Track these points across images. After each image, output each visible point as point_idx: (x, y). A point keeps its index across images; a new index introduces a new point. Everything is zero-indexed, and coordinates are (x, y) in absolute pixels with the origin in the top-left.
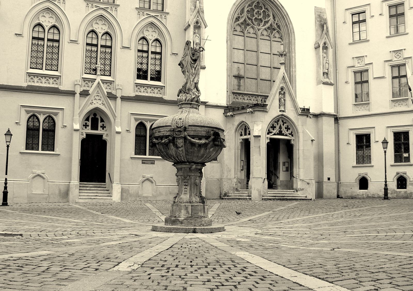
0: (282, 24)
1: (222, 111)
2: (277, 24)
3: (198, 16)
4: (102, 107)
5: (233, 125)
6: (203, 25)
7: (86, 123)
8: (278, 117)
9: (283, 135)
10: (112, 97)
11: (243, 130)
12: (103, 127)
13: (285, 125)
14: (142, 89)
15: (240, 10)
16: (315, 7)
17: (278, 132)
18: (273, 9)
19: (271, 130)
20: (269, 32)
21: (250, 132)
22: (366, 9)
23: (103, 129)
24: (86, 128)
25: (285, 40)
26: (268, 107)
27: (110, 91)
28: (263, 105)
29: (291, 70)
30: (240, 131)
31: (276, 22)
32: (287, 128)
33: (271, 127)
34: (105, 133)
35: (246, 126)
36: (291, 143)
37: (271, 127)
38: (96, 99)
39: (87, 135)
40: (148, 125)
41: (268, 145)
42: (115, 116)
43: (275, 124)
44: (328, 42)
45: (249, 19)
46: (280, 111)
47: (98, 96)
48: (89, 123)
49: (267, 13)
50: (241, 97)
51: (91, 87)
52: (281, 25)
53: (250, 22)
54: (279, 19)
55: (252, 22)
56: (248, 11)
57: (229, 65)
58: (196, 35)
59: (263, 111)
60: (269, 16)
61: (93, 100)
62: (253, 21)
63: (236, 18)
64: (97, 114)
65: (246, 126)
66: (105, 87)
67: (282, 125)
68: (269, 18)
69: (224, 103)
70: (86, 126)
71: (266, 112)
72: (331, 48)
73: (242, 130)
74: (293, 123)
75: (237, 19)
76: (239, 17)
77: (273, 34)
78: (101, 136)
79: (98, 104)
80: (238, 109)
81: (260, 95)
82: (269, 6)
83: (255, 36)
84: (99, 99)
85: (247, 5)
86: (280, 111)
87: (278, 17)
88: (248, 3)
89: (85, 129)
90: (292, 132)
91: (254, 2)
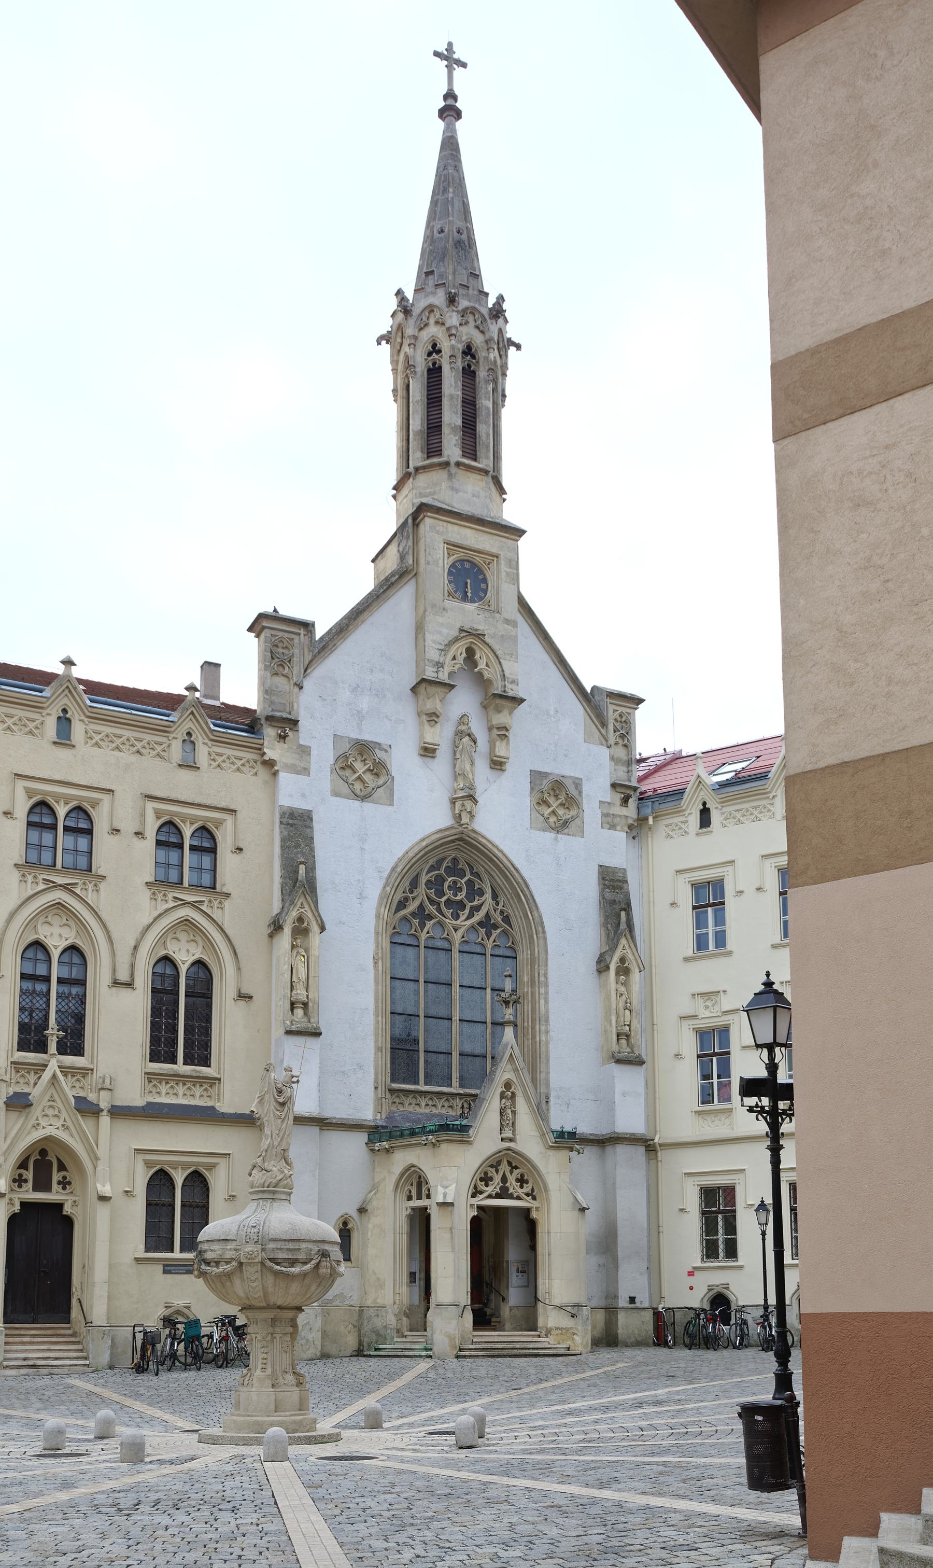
0: (514, 913)
1: (363, 1137)
2: (502, 912)
3: (302, 904)
4: (63, 1135)
5: (389, 1172)
6: (315, 928)
7: (20, 1175)
8: (498, 1155)
9: (511, 1197)
10: (87, 1109)
11: (415, 1184)
12: (64, 1183)
13: (516, 1172)
14: (164, 1088)
15: (410, 879)
16: (600, 866)
18: (491, 875)
19: (481, 1186)
20: (482, 935)
21: (429, 1190)
22: (725, 874)
23: (64, 1188)
24: (20, 1186)
25: (523, 951)
26: (471, 1132)
27: (82, 1094)
28: (459, 1127)
29: (538, 1030)
30: (406, 1189)
31: (500, 907)
32: (522, 1181)
33: (481, 1180)
34: (70, 1198)
35: (420, 1177)
36: (531, 1217)
37: (481, 1180)
38: (47, 1116)
39: (23, 1204)
40: (179, 1179)
41: (476, 1223)
42: (95, 1158)
44: (630, 956)
45: (432, 902)
46: (502, 1140)
47: (51, 1107)
48: (29, 1175)
49: (477, 887)
50: (410, 1099)
51: (35, 1084)
52: (512, 914)
53: (432, 909)
54: (508, 900)
55: (439, 910)
56: (429, 882)
57: (380, 1023)
58: (298, 952)
59: (460, 1141)
60: (481, 893)
61: (40, 1118)
62: (442, 906)
63: (400, 902)
64: (50, 1152)
65: (420, 1177)
66: (69, 1085)
67: (508, 1174)
68: (483, 898)
69: (368, 1113)
70: (19, 1181)
71: (469, 1143)
72: (637, 970)
73: (412, 1185)
74: (534, 1167)
75: (402, 905)
76: (406, 899)
77: (492, 939)
78: (59, 1206)
79: (50, 1128)
80: (402, 1136)
82: (483, 867)
83: (444, 944)
84: (56, 1116)
85: (428, 867)
86: (502, 1140)
87: (506, 896)
88: (431, 862)
89: (18, 1189)
90: (533, 1190)
91: (444, 859)
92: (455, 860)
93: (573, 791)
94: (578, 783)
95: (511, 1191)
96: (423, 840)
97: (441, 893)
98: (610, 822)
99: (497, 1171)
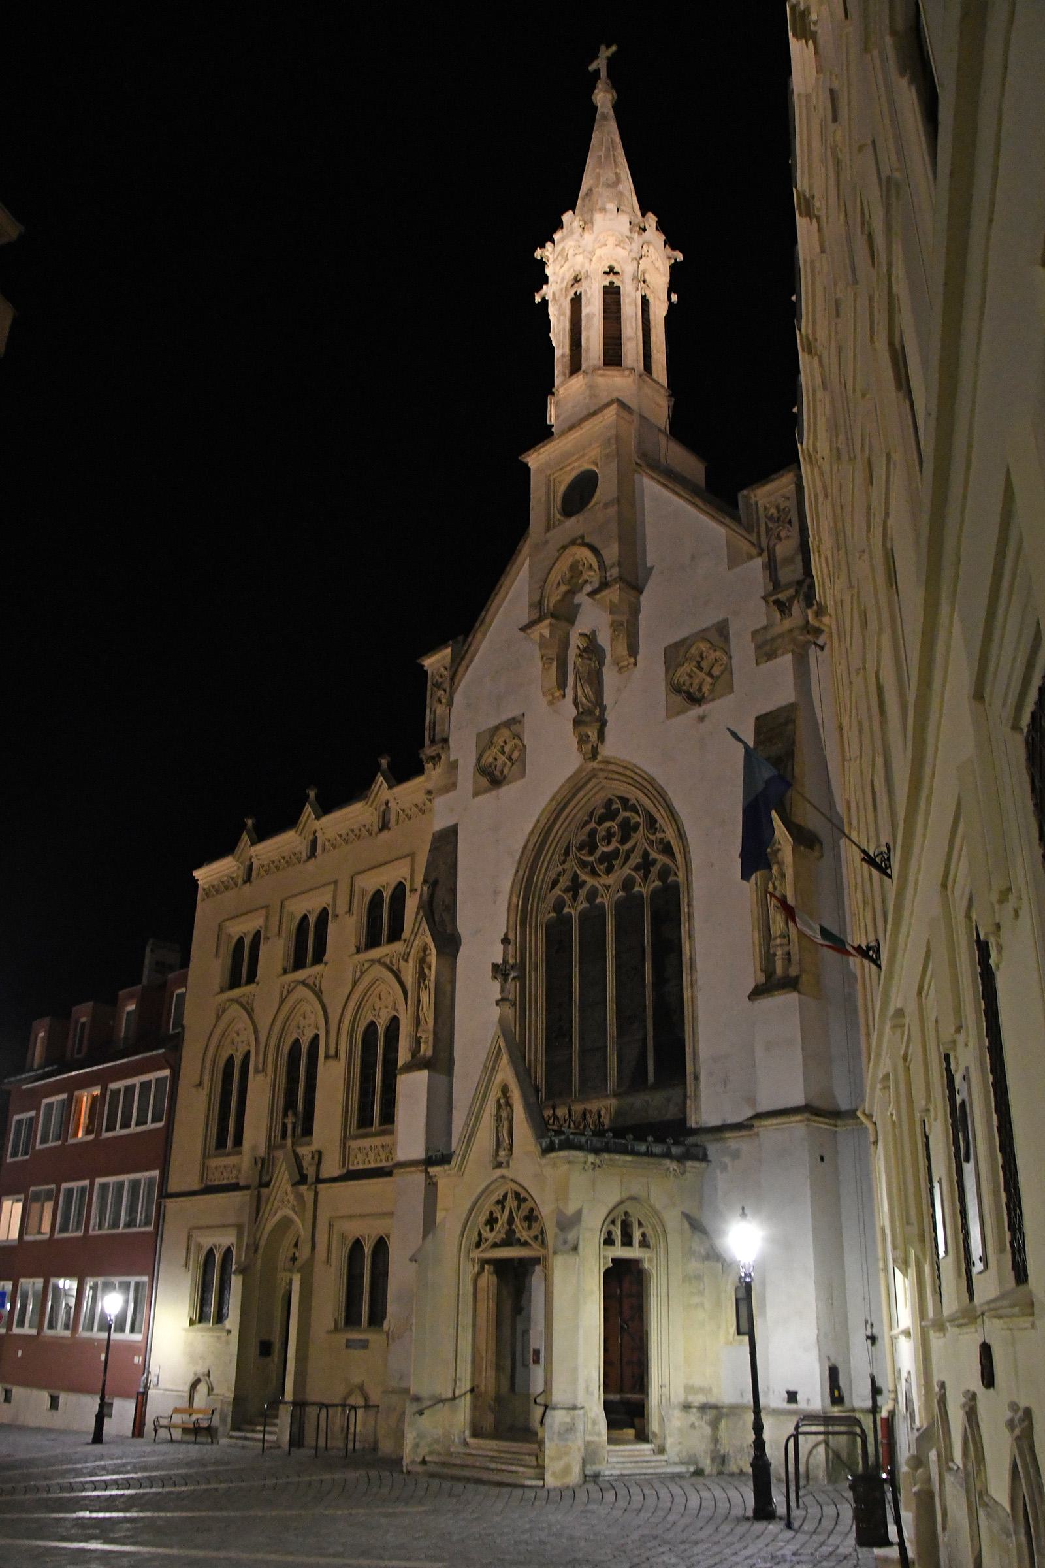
17: (503, 1235)
19: (486, 1234)
45: (583, 864)
90: (542, 1232)
95: (518, 1235)
98: (766, 650)
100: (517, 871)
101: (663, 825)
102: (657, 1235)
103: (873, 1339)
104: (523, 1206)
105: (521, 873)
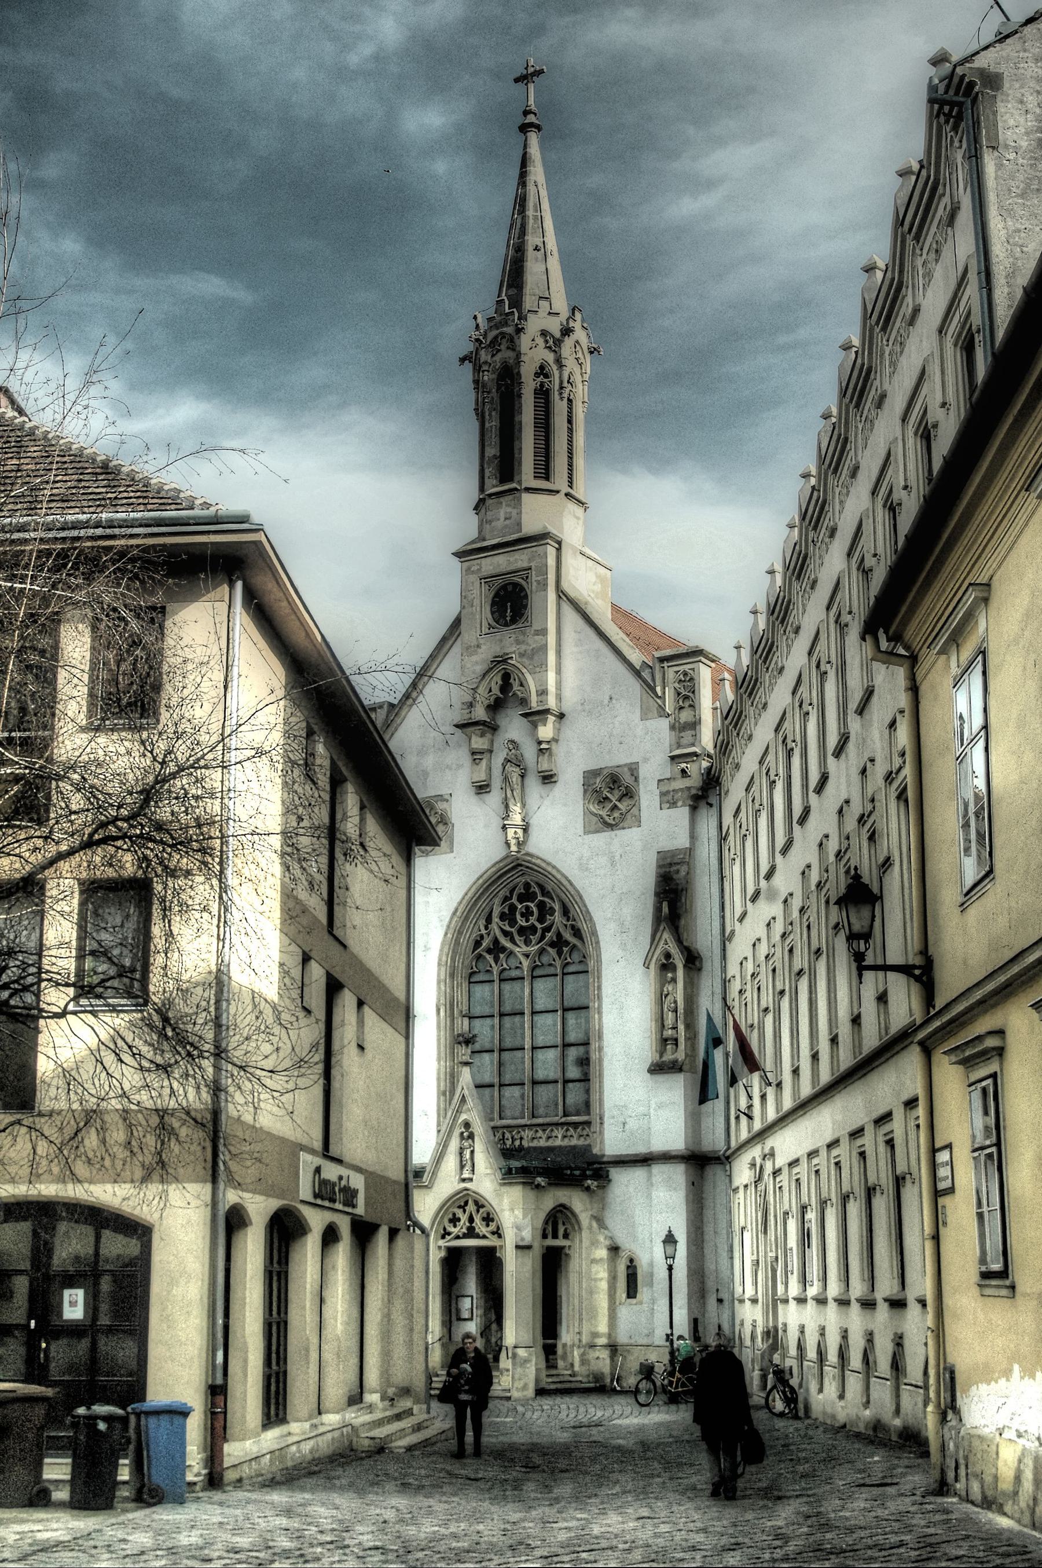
9: (478, 1236)
17: (464, 1230)
33: (451, 1221)
43: (459, 1213)
45: (506, 933)
60: (552, 911)
62: (517, 937)
81: (526, 1126)
88: (502, 894)
90: (498, 1228)
92: (527, 886)
93: (627, 779)
94: (633, 769)
95: (477, 1230)
96: (481, 877)
97: (513, 922)
99: (465, 1211)
100: (446, 934)
101: (576, 916)
102: (573, 1228)
103: (720, 1301)
104: (481, 1210)
105: (449, 936)
